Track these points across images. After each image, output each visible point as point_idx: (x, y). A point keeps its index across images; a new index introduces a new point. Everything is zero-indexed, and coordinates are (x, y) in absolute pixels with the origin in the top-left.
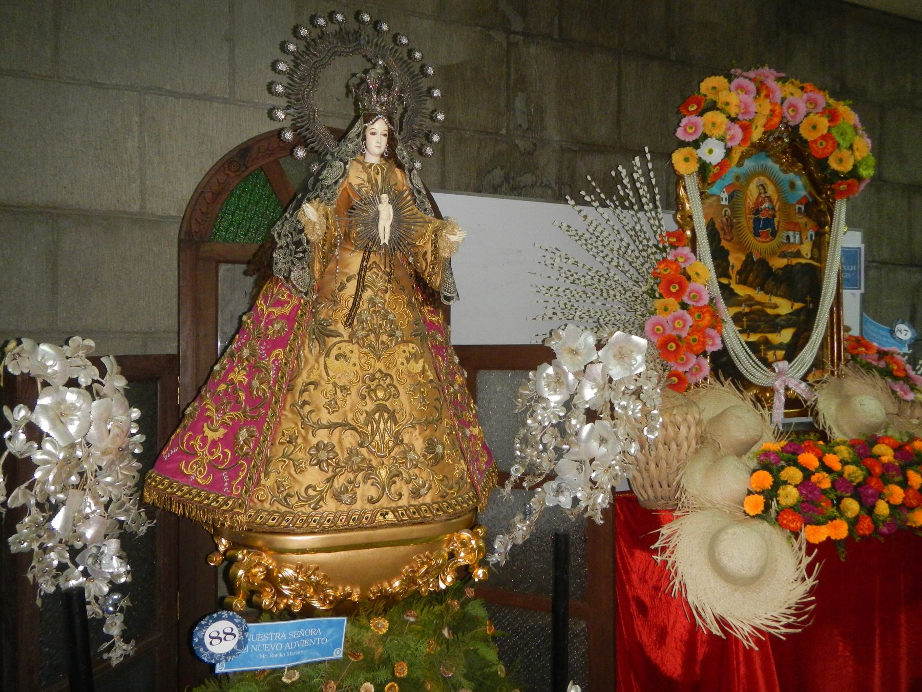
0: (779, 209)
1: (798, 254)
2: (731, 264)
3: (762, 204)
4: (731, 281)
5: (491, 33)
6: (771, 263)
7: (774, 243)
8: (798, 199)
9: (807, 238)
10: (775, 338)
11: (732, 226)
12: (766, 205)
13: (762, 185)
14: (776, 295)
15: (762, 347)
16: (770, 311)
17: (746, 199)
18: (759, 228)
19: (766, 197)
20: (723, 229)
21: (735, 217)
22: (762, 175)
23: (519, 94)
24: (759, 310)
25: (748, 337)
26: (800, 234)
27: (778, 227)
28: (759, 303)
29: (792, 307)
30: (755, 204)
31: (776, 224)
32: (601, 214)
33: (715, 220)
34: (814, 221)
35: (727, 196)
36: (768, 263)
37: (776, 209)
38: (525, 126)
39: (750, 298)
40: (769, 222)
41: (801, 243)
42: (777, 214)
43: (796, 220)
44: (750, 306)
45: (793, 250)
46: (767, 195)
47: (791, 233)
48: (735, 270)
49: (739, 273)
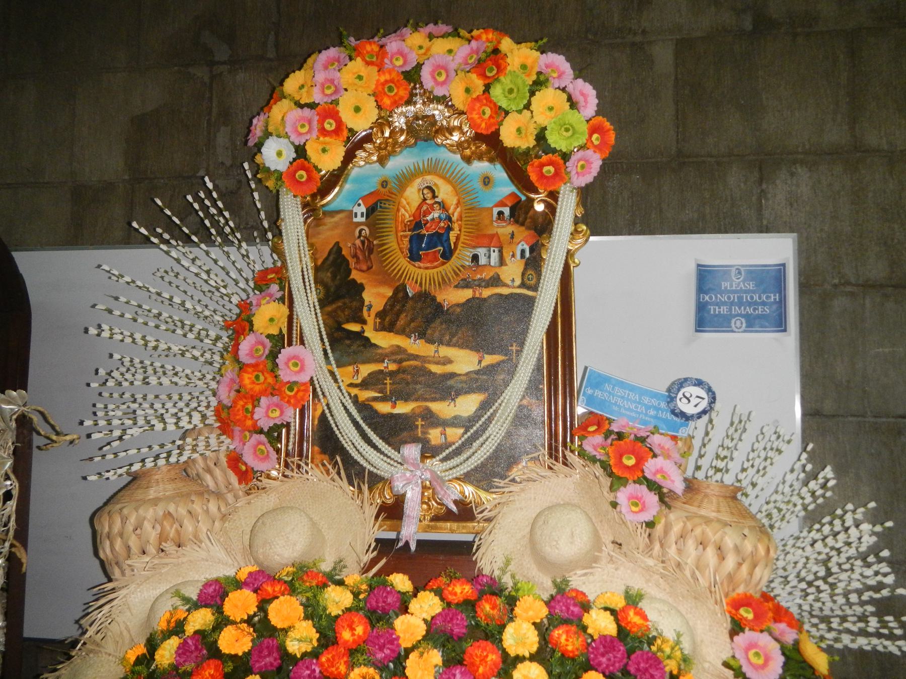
0: (460, 218)
1: (496, 281)
2: (366, 303)
3: (427, 213)
4: (365, 327)
5: (191, 70)
6: (439, 299)
7: (449, 267)
8: (498, 199)
9: (513, 256)
10: (442, 409)
11: (371, 251)
12: (436, 214)
13: (429, 188)
14: (449, 344)
15: (419, 423)
16: (435, 369)
17: (398, 210)
18: (421, 249)
19: (436, 203)
20: (355, 256)
21: (376, 238)
22: (429, 173)
23: (222, 128)
24: (416, 367)
25: (394, 407)
26: (501, 252)
27: (456, 244)
28: (416, 357)
29: (480, 362)
30: (414, 216)
31: (453, 239)
32: (184, 253)
33: (341, 245)
34: (528, 228)
35: (364, 210)
36: (434, 299)
37: (454, 218)
38: (228, 163)
39: (399, 350)
40: (440, 238)
41: (502, 262)
42: (456, 226)
43: (491, 232)
44: (400, 362)
45: (486, 275)
46: (437, 200)
47: (481, 252)
48: (373, 312)
49: (381, 315)
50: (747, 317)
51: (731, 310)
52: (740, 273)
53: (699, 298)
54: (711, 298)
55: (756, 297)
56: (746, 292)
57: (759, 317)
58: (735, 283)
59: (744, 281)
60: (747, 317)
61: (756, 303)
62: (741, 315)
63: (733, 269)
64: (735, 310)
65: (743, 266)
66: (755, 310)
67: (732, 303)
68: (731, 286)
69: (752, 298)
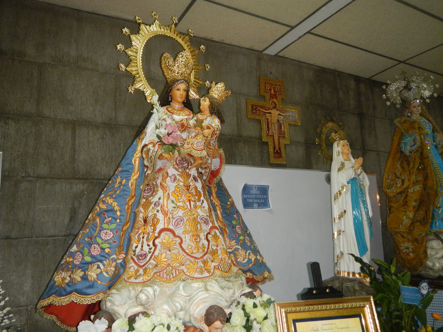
50: (258, 203)
52: (255, 188)
53: (244, 197)
54: (248, 196)
55: (260, 196)
56: (258, 194)
57: (261, 203)
58: (254, 191)
59: (257, 191)
60: (258, 203)
62: (256, 203)
63: (254, 186)
64: (255, 201)
65: (256, 185)
67: (254, 198)
68: (253, 192)
69: (259, 197)
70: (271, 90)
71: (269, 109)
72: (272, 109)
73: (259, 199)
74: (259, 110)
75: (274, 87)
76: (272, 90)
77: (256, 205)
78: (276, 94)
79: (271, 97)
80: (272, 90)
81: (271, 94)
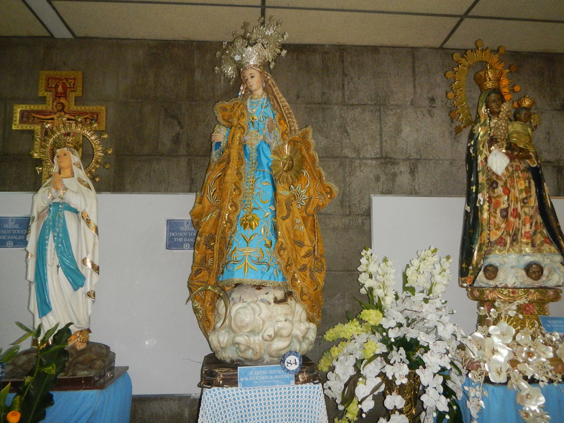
51: (7, 237)
52: (13, 220)
56: (15, 229)
57: (18, 240)
58: (11, 225)
59: (14, 224)
61: (18, 234)
63: (10, 219)
64: (9, 237)
65: (14, 217)
66: (17, 237)
69: (17, 232)
70: (58, 86)
71: (51, 113)
72: (55, 113)
73: (15, 235)
74: (34, 117)
75: (64, 83)
76: (60, 86)
77: (187, 245)
78: (66, 91)
79: (56, 96)
80: (60, 86)
81: (57, 93)
